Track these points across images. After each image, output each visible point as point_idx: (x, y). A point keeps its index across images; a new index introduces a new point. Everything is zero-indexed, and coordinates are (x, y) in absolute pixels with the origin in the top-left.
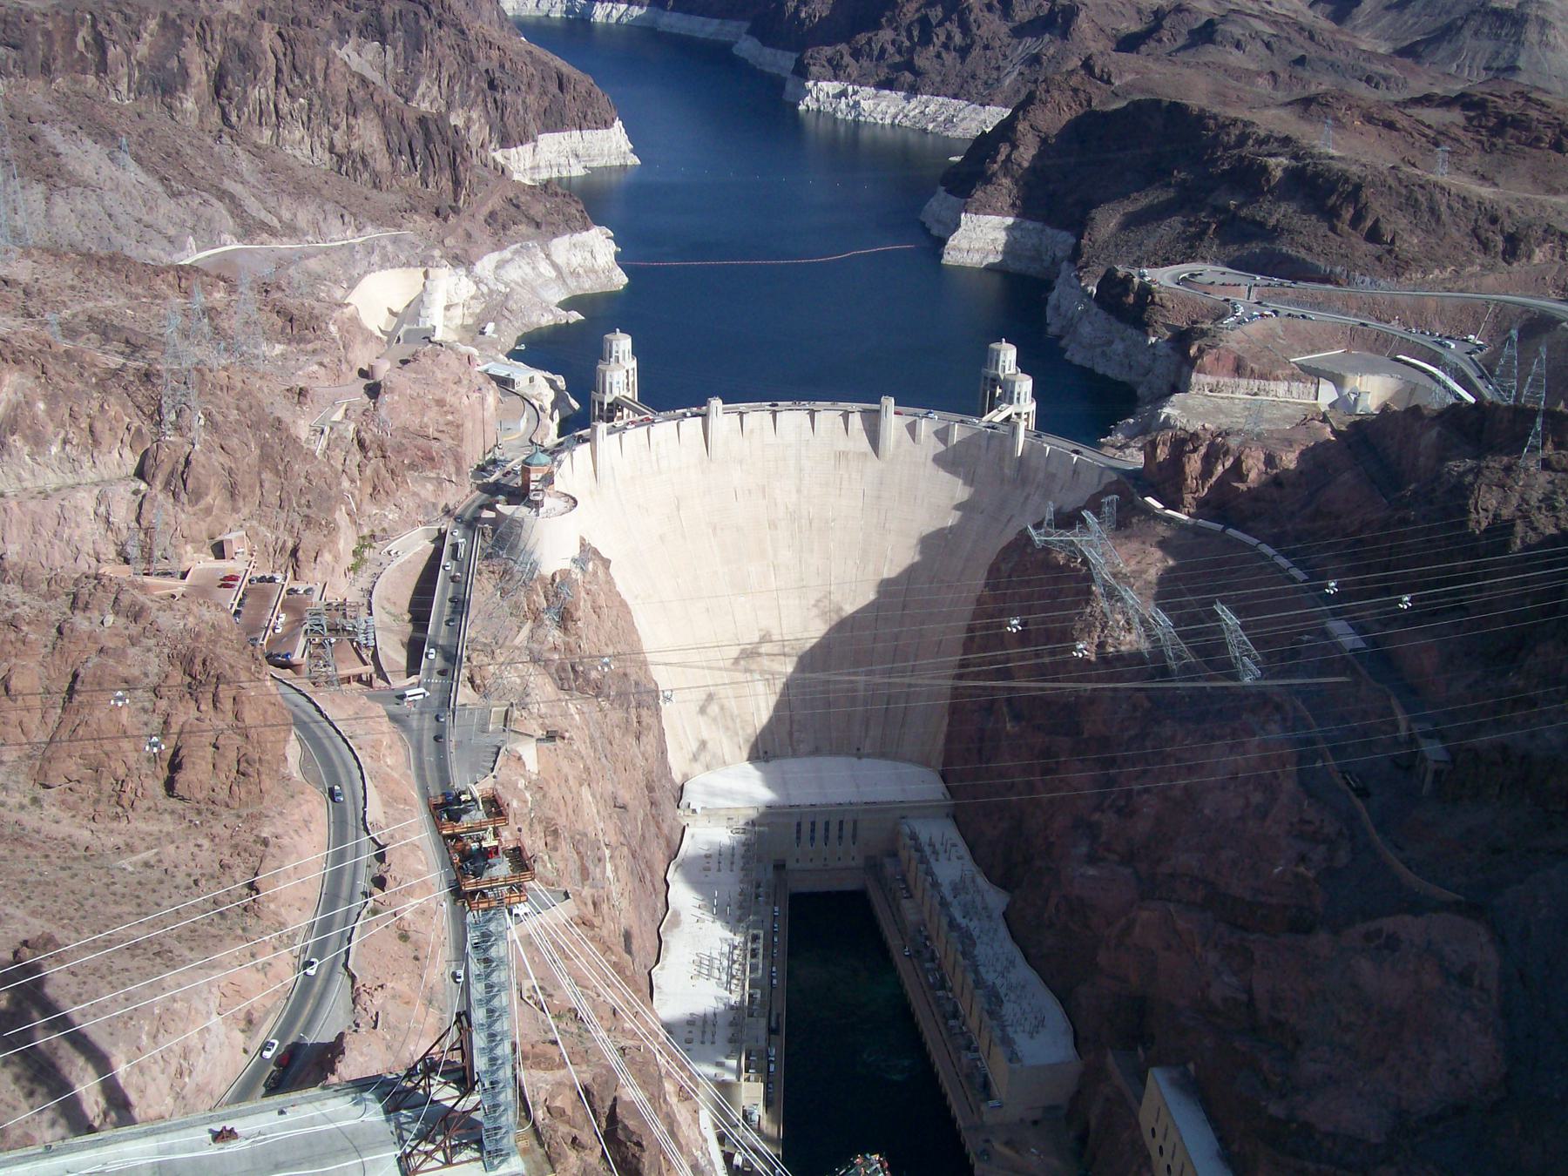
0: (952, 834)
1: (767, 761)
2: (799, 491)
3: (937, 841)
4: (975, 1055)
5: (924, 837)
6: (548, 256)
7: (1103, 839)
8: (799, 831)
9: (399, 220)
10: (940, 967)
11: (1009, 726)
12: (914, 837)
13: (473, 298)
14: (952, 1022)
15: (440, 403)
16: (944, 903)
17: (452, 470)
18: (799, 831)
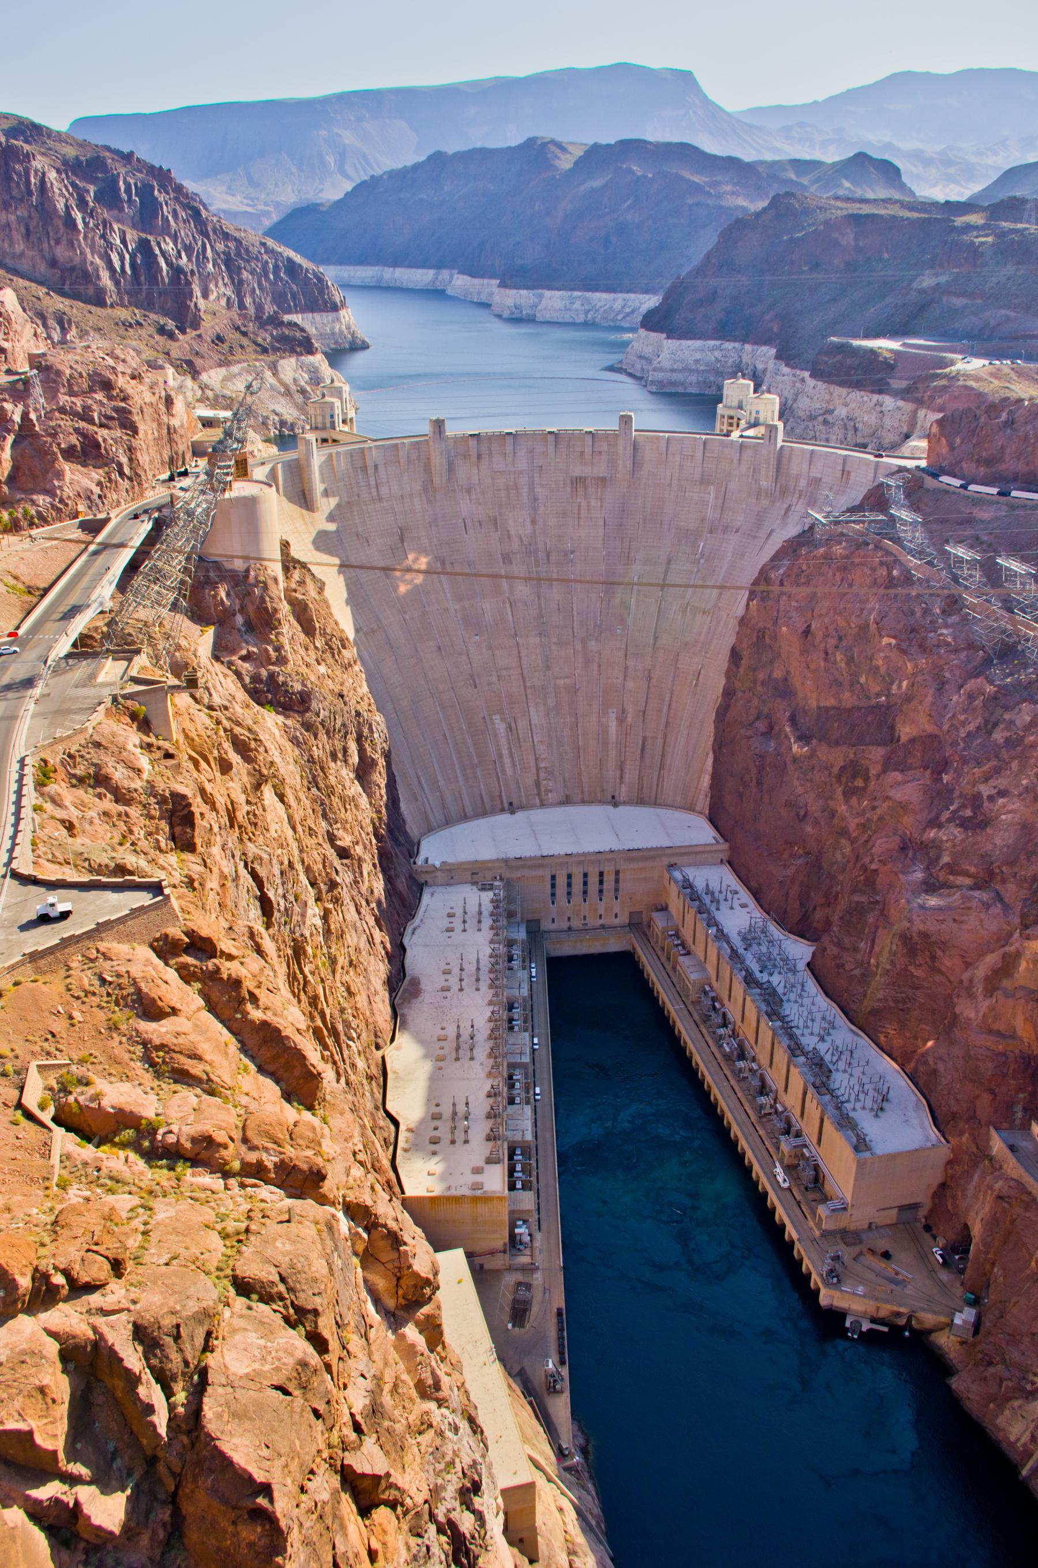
0: (731, 880)
1: (513, 813)
2: (533, 522)
3: (714, 885)
4: (799, 1141)
5: (700, 885)
6: (275, 374)
7: (946, 859)
8: (553, 886)
9: (122, 331)
10: (734, 1034)
11: (795, 748)
12: (687, 884)
14: (763, 1100)
15: (107, 386)
16: (734, 954)
17: (124, 460)
18: (553, 886)
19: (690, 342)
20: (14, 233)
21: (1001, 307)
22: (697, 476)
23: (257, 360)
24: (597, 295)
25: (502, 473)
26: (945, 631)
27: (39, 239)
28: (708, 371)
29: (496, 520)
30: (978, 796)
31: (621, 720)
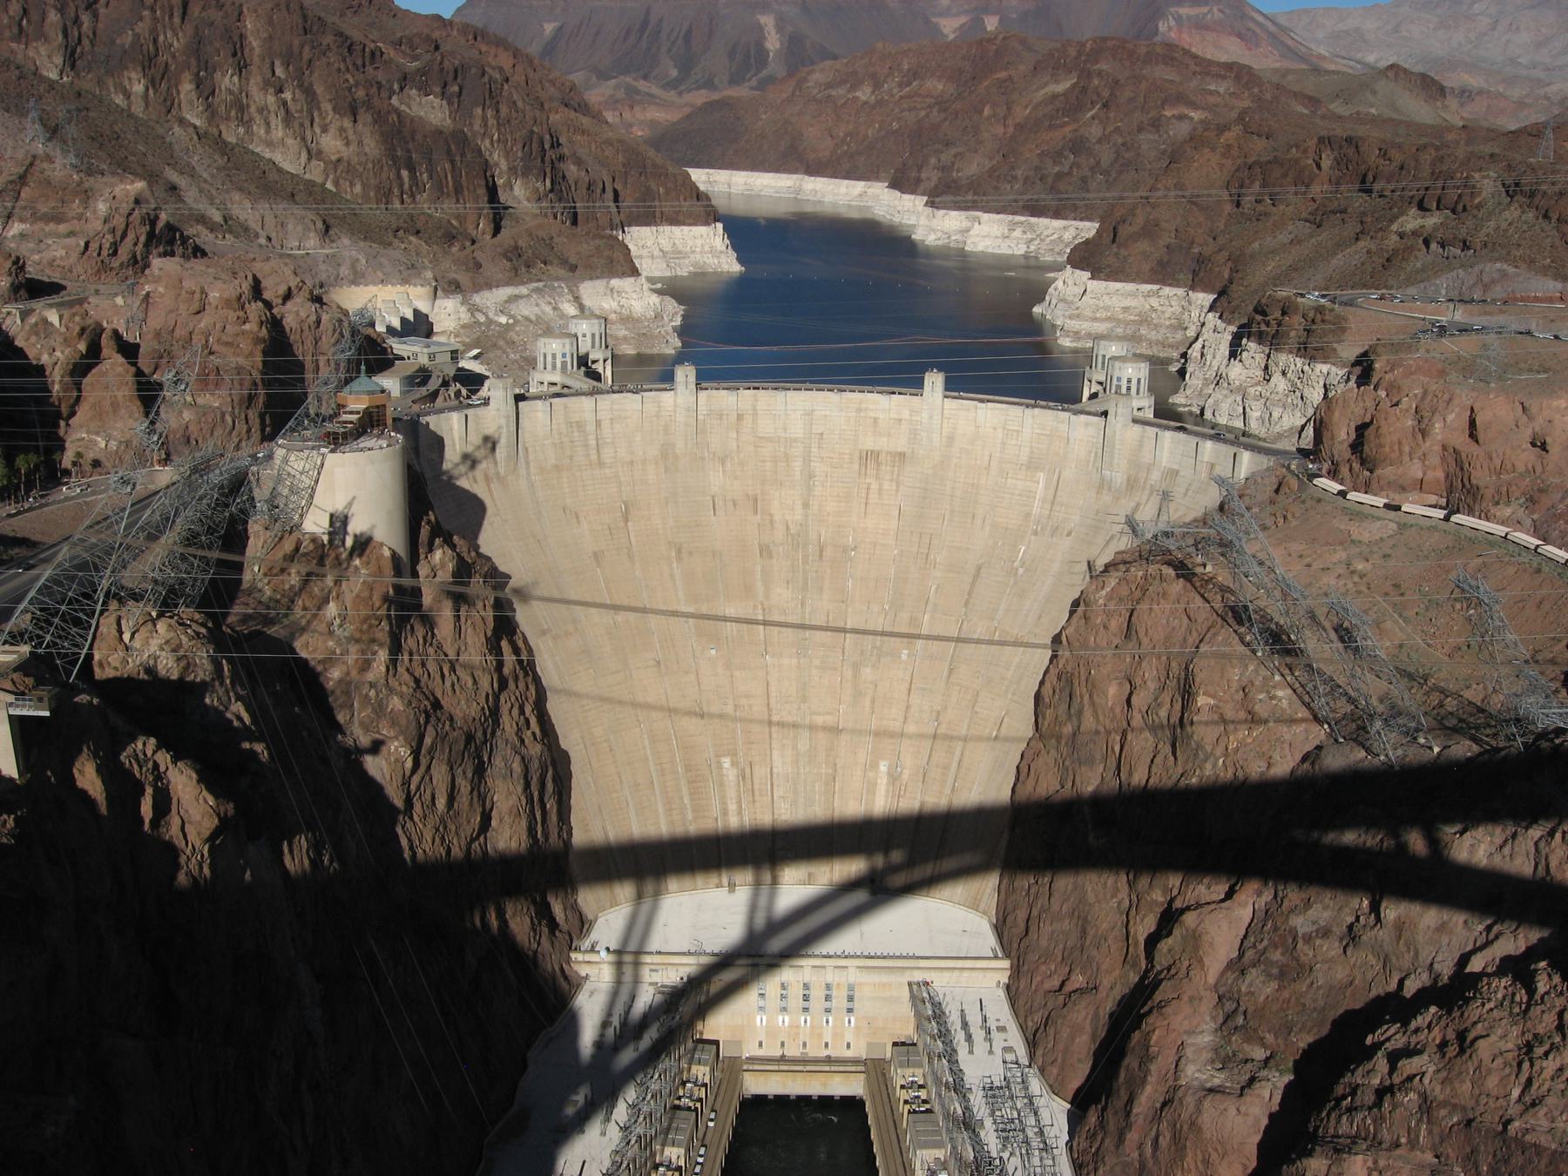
0: (1000, 1011)
2: (806, 505)
6: (577, 299)
13: (463, 327)
19: (1119, 285)
20: (272, 118)
21: (1497, 260)
22: (1024, 458)
23: (557, 279)
24: (1044, 221)
25: (769, 440)
26: (1280, 693)
27: (302, 125)
28: (1141, 323)
29: (756, 500)
30: (1294, 933)
31: (893, 778)
